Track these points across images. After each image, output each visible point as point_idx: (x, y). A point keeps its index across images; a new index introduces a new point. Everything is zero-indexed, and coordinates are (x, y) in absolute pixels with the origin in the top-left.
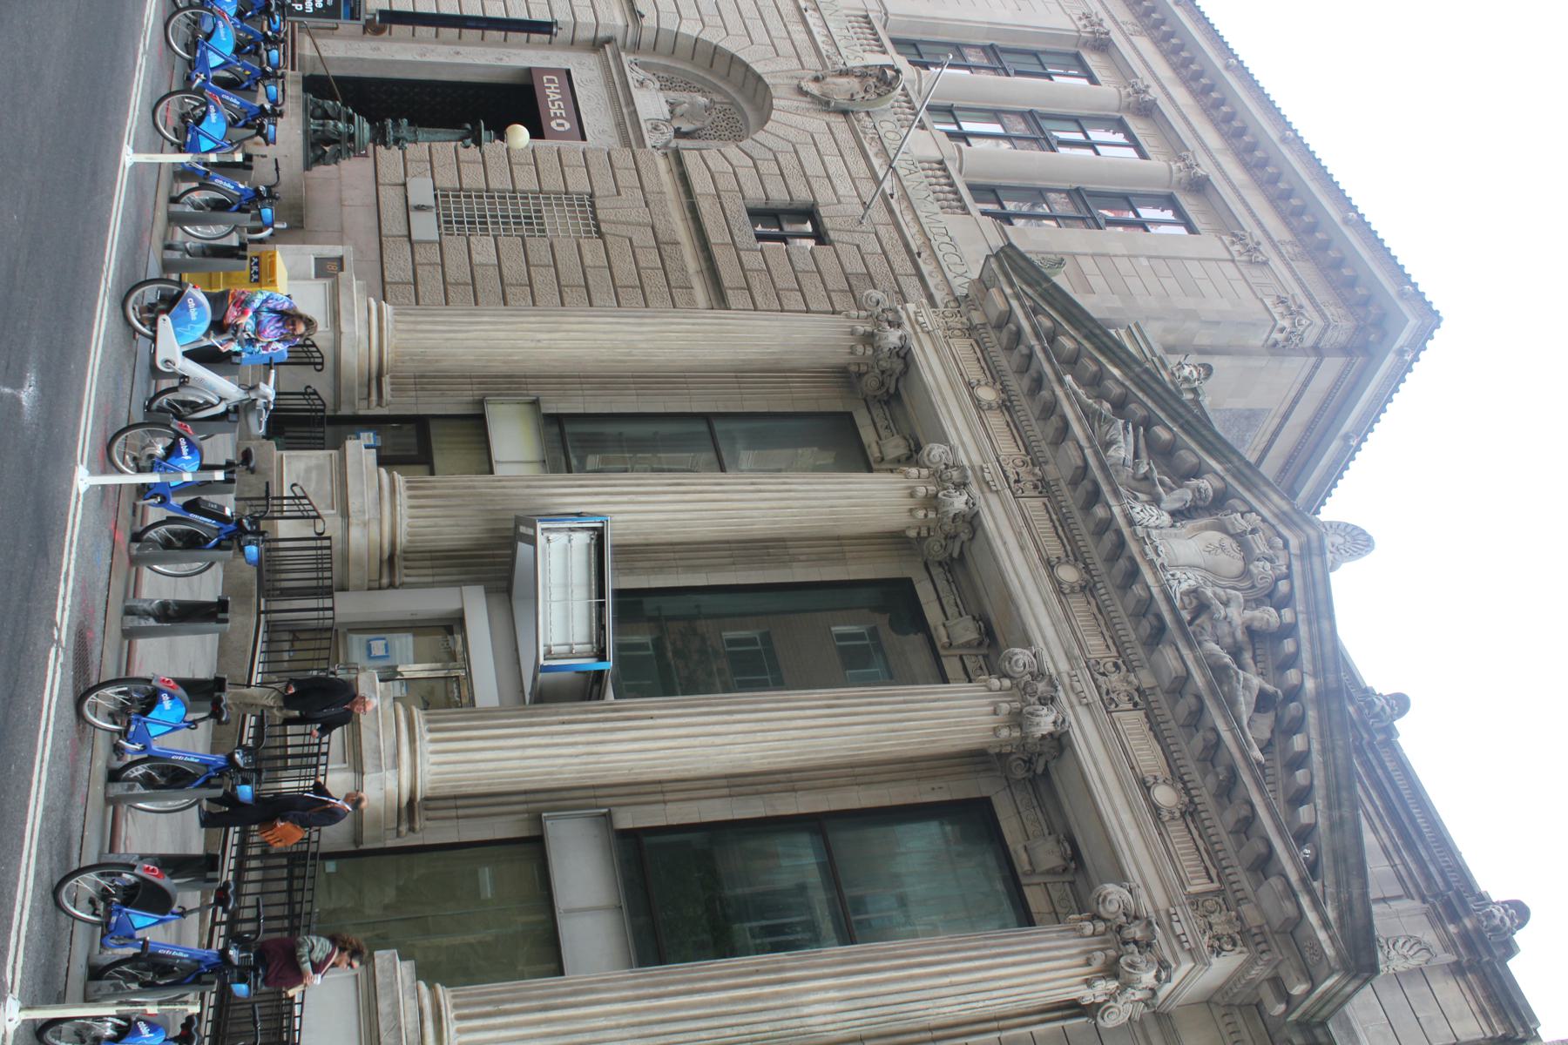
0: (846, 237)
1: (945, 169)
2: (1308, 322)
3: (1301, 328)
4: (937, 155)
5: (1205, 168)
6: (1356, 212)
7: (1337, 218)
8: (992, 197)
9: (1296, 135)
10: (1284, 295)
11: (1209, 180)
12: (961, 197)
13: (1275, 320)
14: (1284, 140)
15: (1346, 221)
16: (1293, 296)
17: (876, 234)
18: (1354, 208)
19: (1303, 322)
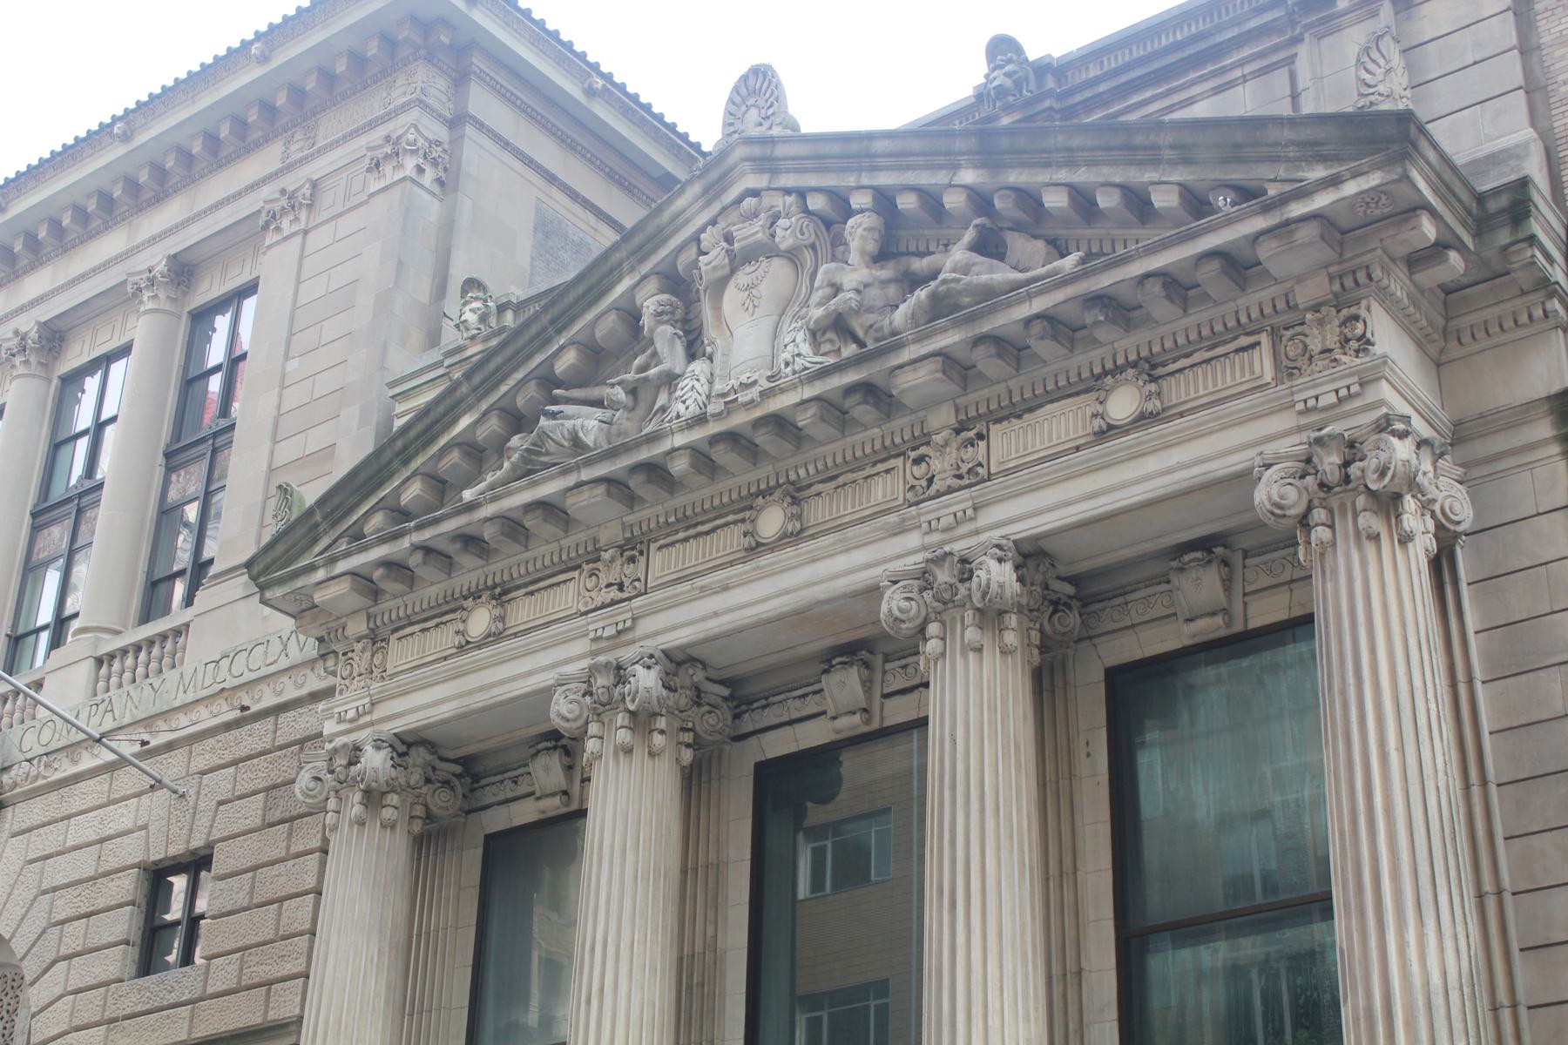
0: (203, 821)
1: (112, 656)
2: (412, 130)
3: (421, 141)
4: (89, 665)
5: (156, 259)
6: (251, 43)
7: (256, 72)
8: (162, 588)
9: (121, 119)
10: (367, 161)
11: (175, 256)
12: (159, 635)
13: (404, 179)
14: (126, 138)
15: (264, 59)
16: (369, 149)
17: (204, 773)
18: (245, 45)
19: (411, 137)
